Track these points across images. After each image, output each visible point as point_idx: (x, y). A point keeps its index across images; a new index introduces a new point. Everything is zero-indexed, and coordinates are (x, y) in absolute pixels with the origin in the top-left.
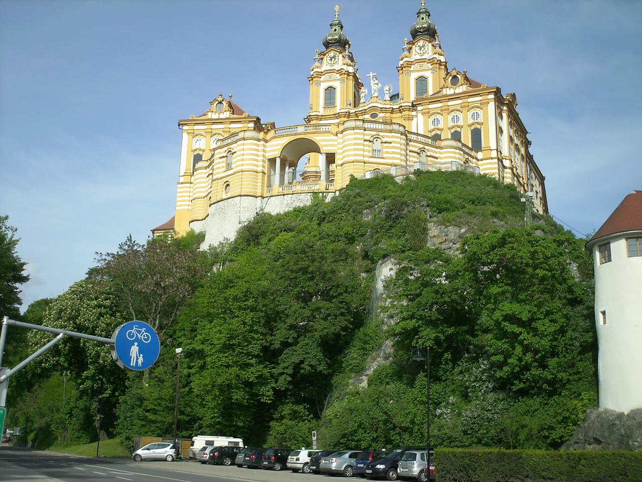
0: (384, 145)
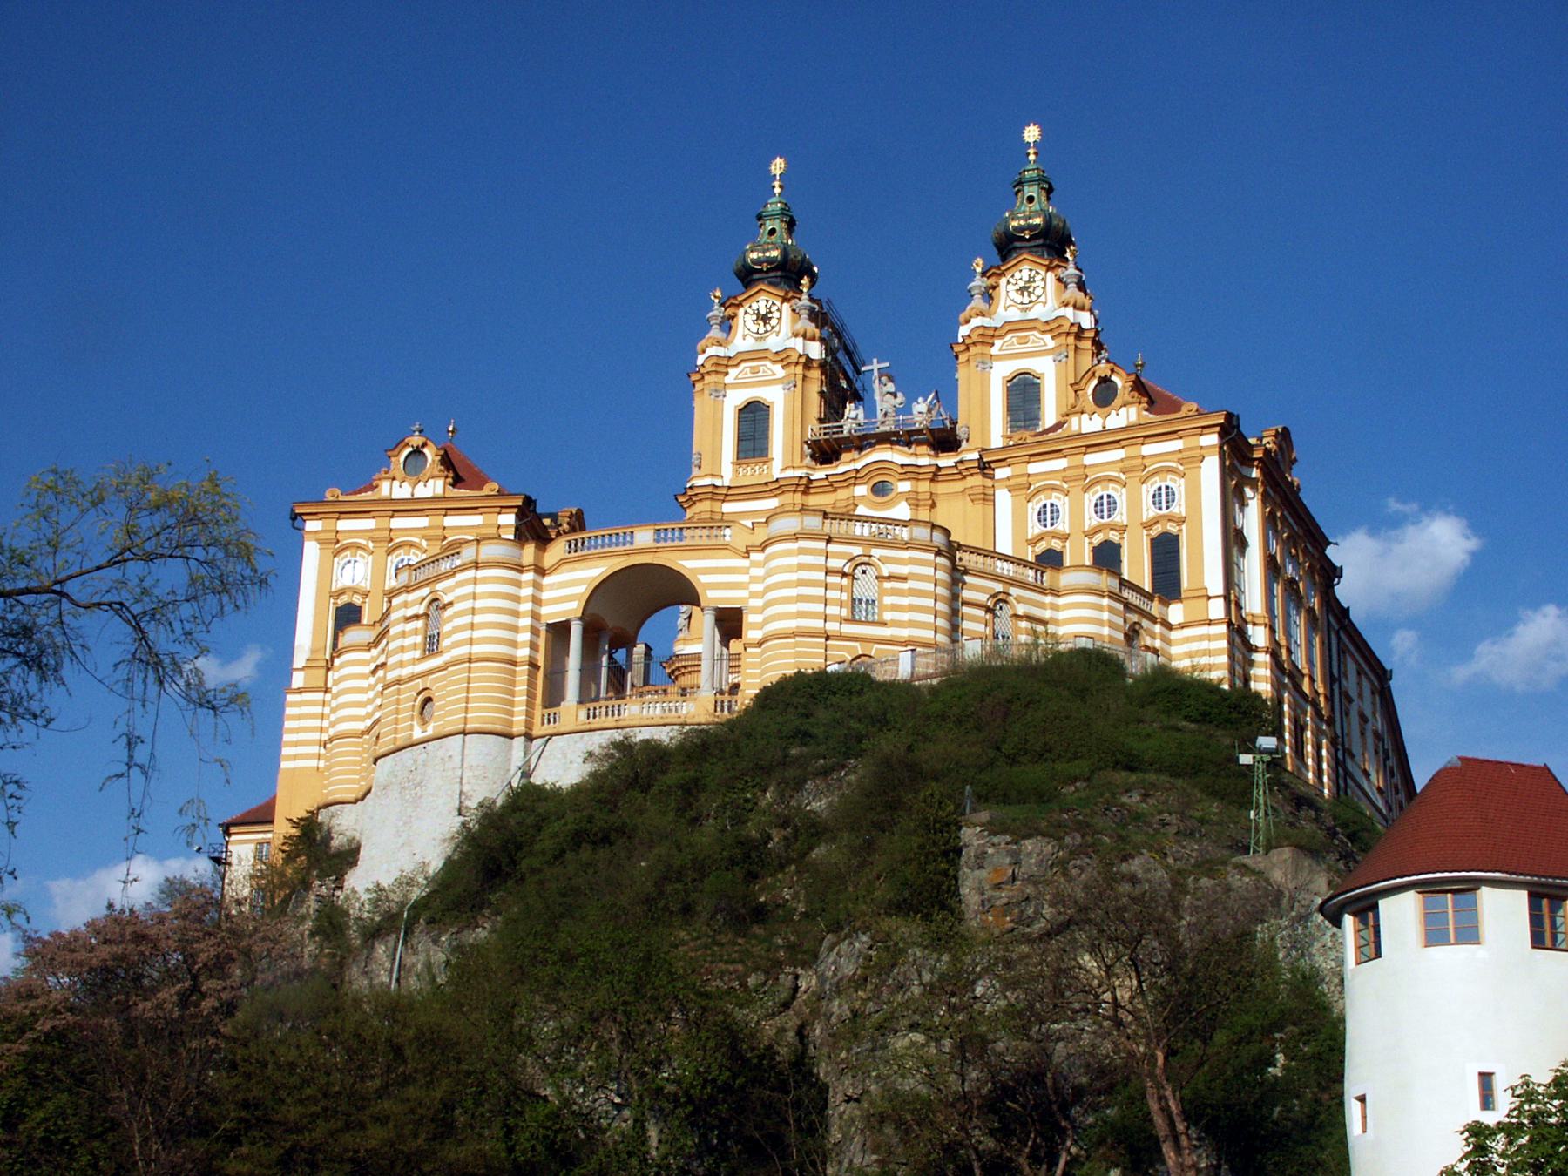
0: (887, 585)
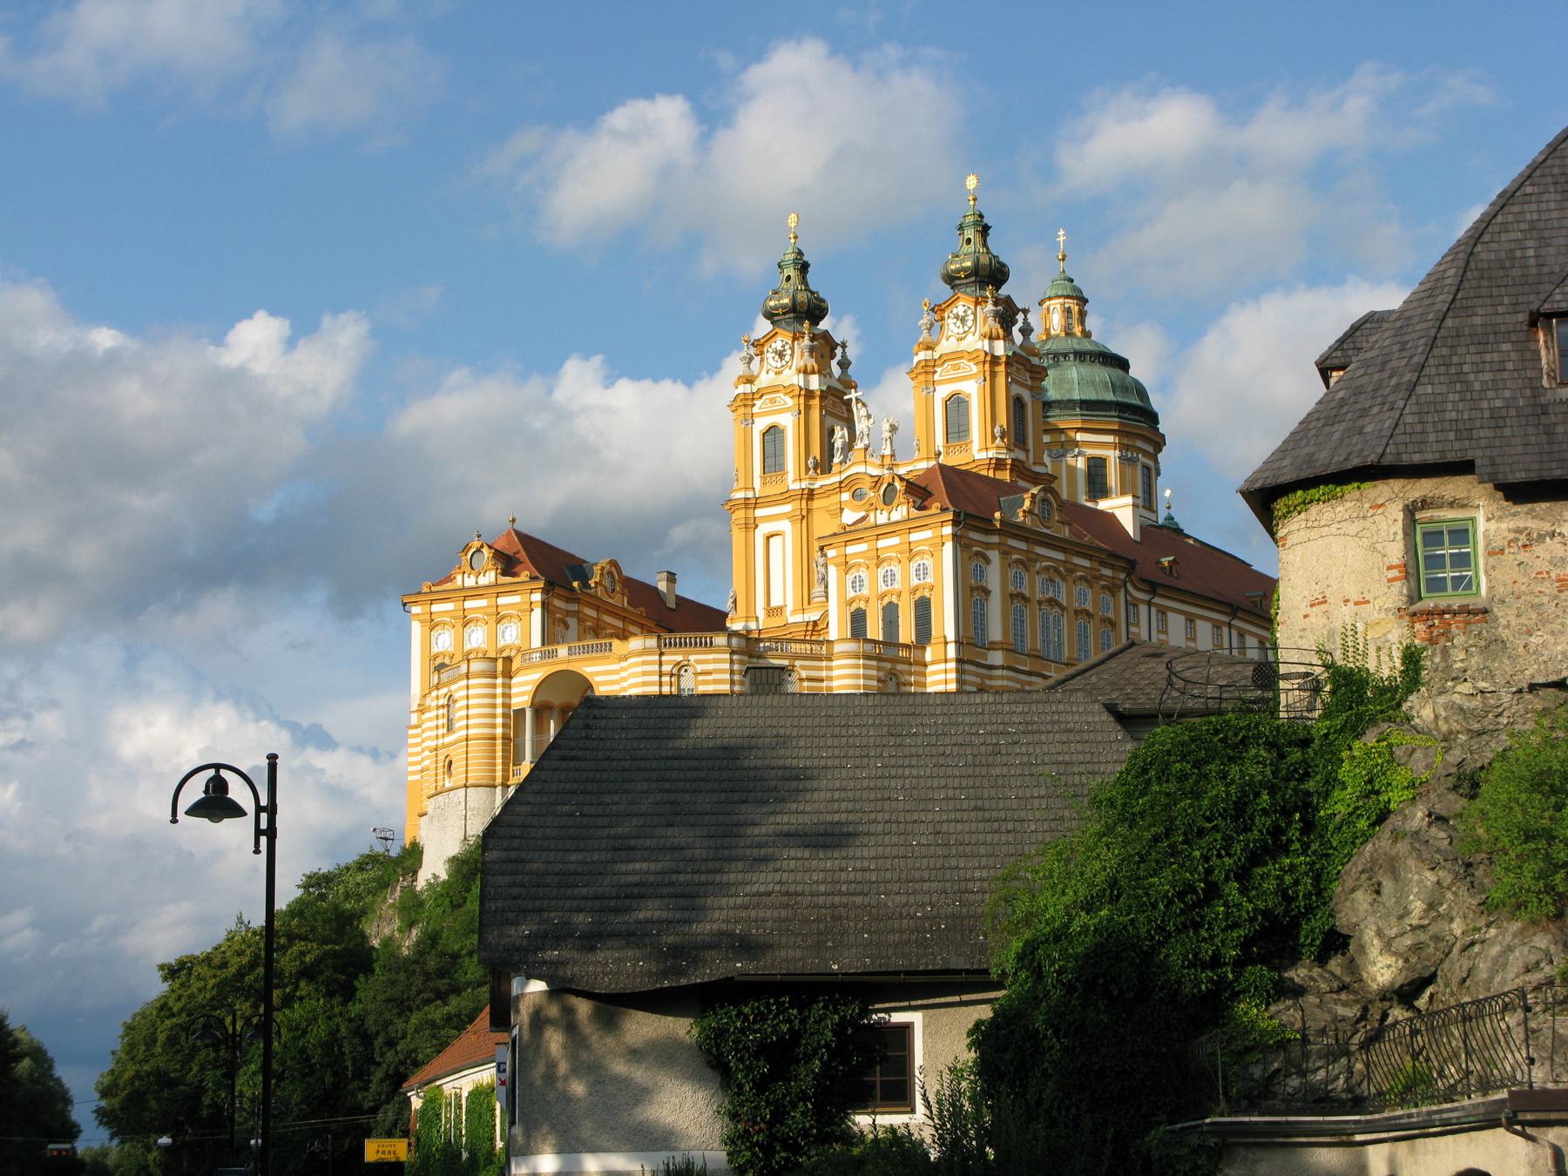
0: (700, 678)
